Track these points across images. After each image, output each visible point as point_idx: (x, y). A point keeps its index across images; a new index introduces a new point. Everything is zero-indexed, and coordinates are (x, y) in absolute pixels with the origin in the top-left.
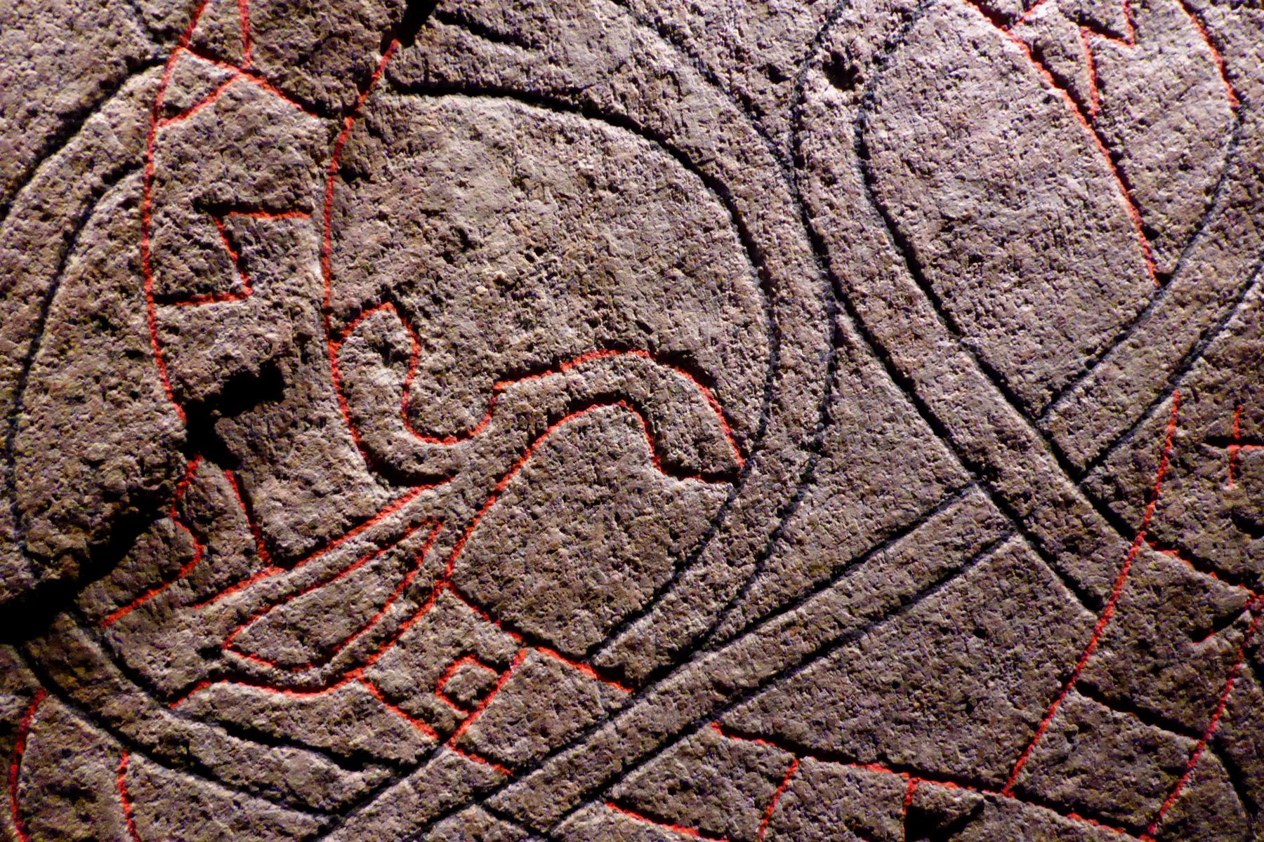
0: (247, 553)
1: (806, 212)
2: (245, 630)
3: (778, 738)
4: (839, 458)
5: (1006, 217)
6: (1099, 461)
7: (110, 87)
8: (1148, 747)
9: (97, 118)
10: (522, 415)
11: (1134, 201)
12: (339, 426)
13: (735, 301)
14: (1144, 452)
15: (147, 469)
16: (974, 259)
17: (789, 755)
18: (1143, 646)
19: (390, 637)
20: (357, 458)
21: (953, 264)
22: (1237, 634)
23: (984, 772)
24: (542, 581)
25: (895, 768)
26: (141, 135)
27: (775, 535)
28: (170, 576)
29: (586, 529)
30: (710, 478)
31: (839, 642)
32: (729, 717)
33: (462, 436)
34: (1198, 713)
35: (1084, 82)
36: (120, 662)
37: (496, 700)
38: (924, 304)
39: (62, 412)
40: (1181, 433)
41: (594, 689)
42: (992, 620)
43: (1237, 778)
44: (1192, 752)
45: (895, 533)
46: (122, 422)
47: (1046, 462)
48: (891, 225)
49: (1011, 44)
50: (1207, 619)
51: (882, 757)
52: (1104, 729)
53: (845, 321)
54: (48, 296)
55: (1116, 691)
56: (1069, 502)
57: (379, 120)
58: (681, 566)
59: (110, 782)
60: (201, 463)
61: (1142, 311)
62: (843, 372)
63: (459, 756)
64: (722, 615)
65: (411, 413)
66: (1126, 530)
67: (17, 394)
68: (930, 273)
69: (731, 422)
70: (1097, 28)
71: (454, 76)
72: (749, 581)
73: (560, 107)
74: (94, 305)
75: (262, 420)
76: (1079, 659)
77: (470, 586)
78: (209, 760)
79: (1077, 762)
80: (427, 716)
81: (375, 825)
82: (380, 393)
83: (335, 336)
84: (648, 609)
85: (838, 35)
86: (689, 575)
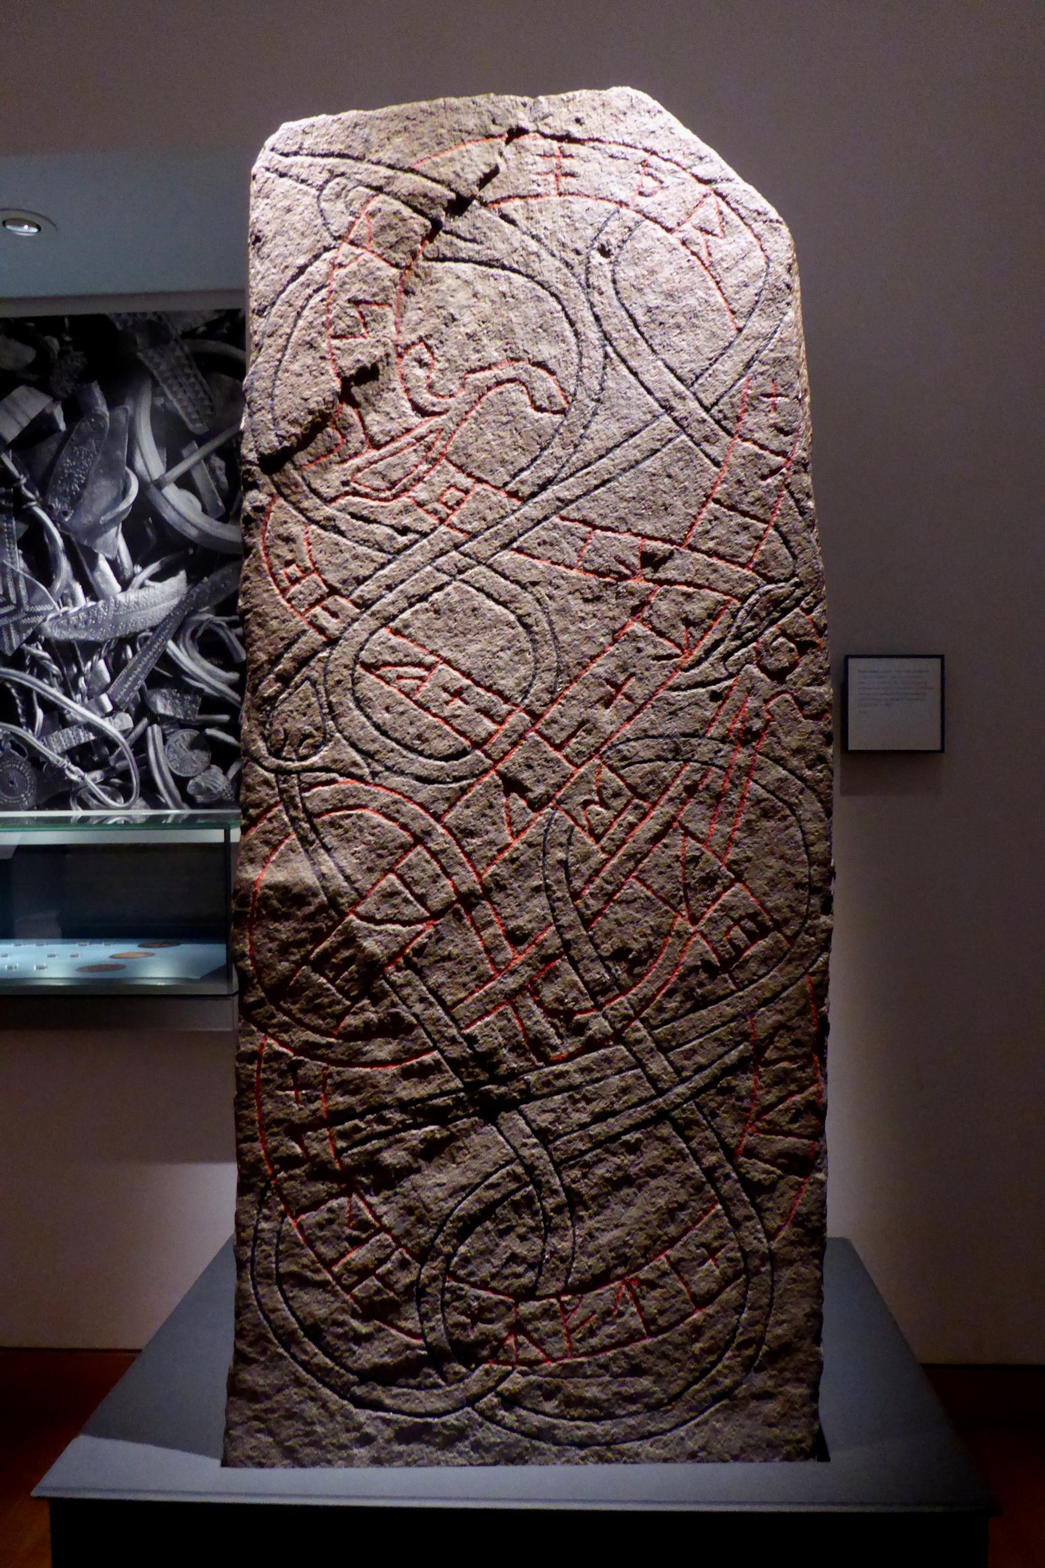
0: (362, 443)
1: (592, 306)
2: (360, 475)
3: (585, 522)
4: (608, 405)
5: (673, 307)
6: (716, 404)
7: (316, 257)
8: (746, 528)
9: (310, 269)
10: (476, 387)
11: (726, 300)
12: (400, 391)
13: (563, 341)
14: (734, 400)
15: (325, 402)
16: (661, 323)
17: (589, 529)
18: (739, 482)
19: (419, 479)
20: (408, 405)
21: (652, 326)
22: (780, 478)
23: (673, 537)
24: (484, 455)
25: (636, 535)
26: (328, 275)
27: (581, 437)
28: (330, 451)
29: (502, 434)
30: (555, 413)
31: (609, 480)
32: (563, 513)
33: (451, 396)
34: (765, 512)
35: (703, 254)
36: (309, 486)
37: (464, 506)
38: (641, 342)
39: (293, 379)
40: (750, 392)
41: (505, 501)
42: (674, 470)
43: (786, 542)
44: (765, 530)
45: (633, 435)
46: (317, 384)
47: (694, 405)
48: (627, 311)
49: (674, 239)
50: (766, 471)
51: (629, 530)
52: (726, 519)
53: (609, 349)
54: (290, 335)
55: (728, 502)
56: (704, 421)
57: (419, 271)
58: (542, 449)
59: (302, 536)
60: (344, 406)
61: (731, 343)
62: (608, 369)
63: (448, 529)
64: (560, 470)
65: (430, 387)
66: (728, 433)
67: (276, 373)
68: (643, 329)
69: (563, 389)
70: (708, 232)
71: (449, 254)
72: (571, 455)
73: (491, 266)
74: (308, 339)
75: (369, 388)
76: (712, 488)
77: (454, 458)
78: (343, 528)
79: (714, 534)
80: (435, 512)
81: (412, 559)
82: (418, 379)
83: (400, 356)
84: (528, 467)
85: (603, 238)
86: (546, 453)
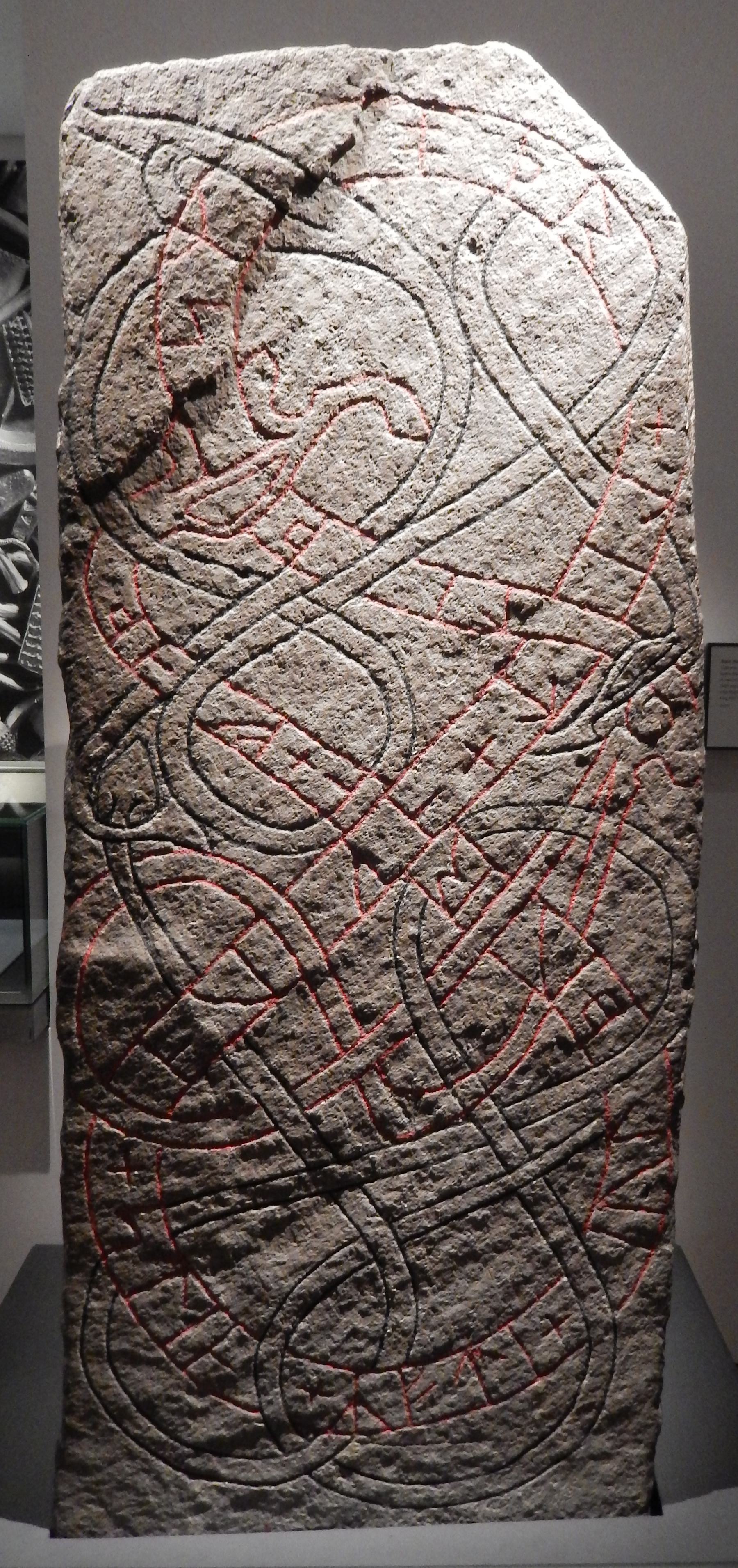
0: (197, 468)
2: (194, 506)
3: (446, 566)
5: (552, 317)
6: (595, 434)
7: (141, 244)
8: (621, 576)
9: (135, 258)
10: (327, 406)
12: (240, 408)
13: (426, 354)
14: (615, 430)
15: (155, 421)
16: (537, 337)
18: (617, 525)
19: (262, 512)
20: (249, 424)
21: (527, 339)
22: (662, 520)
23: (543, 585)
24: (336, 486)
25: (503, 582)
26: (157, 267)
27: (445, 468)
28: (161, 477)
29: (356, 462)
30: (416, 439)
31: (474, 520)
32: (423, 555)
33: (299, 415)
34: (644, 560)
35: (587, 254)
36: (137, 518)
37: (311, 544)
39: (118, 393)
40: (632, 421)
42: (546, 510)
43: (665, 593)
44: (643, 579)
46: (145, 400)
49: (554, 235)
50: (646, 513)
51: (495, 577)
54: (112, 339)
55: (604, 547)
56: (582, 454)
57: (262, 264)
58: (401, 481)
60: (176, 424)
61: (614, 363)
62: (476, 389)
63: (295, 571)
65: (275, 403)
66: (608, 468)
67: (97, 385)
68: (516, 343)
69: (425, 412)
70: (593, 229)
71: (296, 244)
72: (433, 490)
73: (345, 260)
74: (134, 344)
75: (206, 403)
77: (301, 488)
78: (177, 568)
79: (588, 582)
80: (280, 551)
81: (254, 604)
82: (261, 395)
83: (240, 365)
85: (473, 231)
86: (405, 486)
